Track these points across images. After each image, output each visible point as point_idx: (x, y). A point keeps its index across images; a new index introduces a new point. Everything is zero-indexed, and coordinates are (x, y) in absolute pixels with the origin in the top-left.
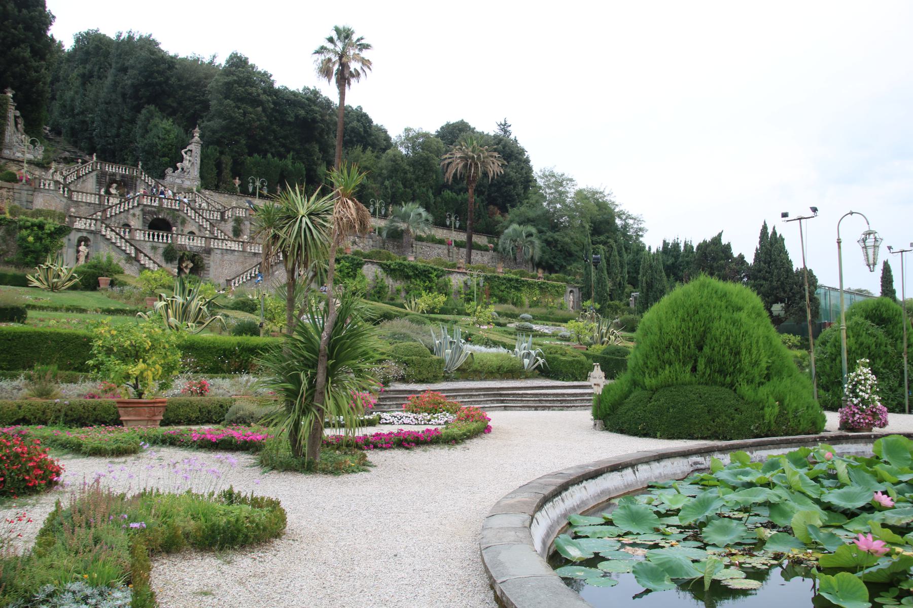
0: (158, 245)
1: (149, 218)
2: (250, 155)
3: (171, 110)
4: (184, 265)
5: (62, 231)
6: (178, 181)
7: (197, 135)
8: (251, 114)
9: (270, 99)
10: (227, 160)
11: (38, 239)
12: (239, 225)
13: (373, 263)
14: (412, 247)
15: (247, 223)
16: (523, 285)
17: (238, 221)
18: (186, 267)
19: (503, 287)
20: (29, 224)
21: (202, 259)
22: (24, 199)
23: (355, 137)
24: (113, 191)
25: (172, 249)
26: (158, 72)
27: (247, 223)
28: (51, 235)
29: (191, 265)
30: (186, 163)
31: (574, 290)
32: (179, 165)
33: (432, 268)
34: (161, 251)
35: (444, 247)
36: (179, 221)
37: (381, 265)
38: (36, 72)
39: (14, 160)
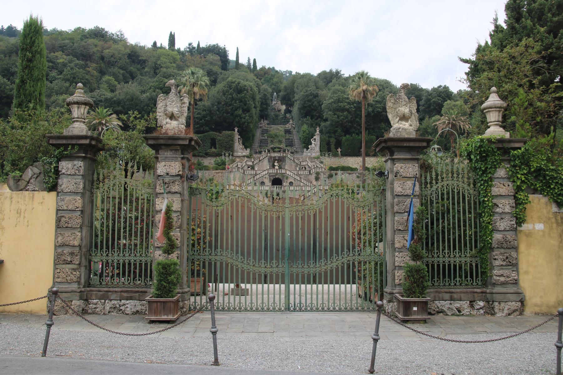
1: (272, 178)
6: (309, 154)
7: (318, 131)
8: (341, 116)
9: (352, 106)
10: (333, 140)
12: (318, 175)
15: (322, 174)
17: (318, 174)
24: (276, 164)
26: (309, 101)
27: (322, 174)
30: (313, 145)
32: (309, 146)
36: (285, 178)
38: (244, 118)
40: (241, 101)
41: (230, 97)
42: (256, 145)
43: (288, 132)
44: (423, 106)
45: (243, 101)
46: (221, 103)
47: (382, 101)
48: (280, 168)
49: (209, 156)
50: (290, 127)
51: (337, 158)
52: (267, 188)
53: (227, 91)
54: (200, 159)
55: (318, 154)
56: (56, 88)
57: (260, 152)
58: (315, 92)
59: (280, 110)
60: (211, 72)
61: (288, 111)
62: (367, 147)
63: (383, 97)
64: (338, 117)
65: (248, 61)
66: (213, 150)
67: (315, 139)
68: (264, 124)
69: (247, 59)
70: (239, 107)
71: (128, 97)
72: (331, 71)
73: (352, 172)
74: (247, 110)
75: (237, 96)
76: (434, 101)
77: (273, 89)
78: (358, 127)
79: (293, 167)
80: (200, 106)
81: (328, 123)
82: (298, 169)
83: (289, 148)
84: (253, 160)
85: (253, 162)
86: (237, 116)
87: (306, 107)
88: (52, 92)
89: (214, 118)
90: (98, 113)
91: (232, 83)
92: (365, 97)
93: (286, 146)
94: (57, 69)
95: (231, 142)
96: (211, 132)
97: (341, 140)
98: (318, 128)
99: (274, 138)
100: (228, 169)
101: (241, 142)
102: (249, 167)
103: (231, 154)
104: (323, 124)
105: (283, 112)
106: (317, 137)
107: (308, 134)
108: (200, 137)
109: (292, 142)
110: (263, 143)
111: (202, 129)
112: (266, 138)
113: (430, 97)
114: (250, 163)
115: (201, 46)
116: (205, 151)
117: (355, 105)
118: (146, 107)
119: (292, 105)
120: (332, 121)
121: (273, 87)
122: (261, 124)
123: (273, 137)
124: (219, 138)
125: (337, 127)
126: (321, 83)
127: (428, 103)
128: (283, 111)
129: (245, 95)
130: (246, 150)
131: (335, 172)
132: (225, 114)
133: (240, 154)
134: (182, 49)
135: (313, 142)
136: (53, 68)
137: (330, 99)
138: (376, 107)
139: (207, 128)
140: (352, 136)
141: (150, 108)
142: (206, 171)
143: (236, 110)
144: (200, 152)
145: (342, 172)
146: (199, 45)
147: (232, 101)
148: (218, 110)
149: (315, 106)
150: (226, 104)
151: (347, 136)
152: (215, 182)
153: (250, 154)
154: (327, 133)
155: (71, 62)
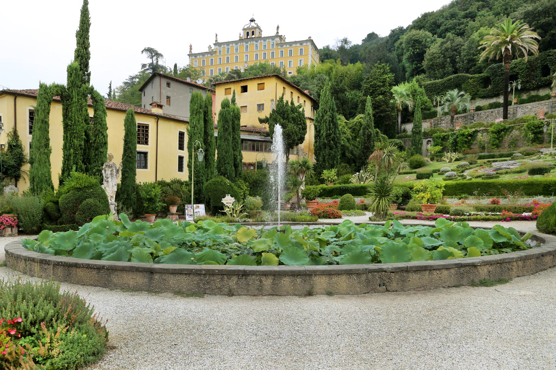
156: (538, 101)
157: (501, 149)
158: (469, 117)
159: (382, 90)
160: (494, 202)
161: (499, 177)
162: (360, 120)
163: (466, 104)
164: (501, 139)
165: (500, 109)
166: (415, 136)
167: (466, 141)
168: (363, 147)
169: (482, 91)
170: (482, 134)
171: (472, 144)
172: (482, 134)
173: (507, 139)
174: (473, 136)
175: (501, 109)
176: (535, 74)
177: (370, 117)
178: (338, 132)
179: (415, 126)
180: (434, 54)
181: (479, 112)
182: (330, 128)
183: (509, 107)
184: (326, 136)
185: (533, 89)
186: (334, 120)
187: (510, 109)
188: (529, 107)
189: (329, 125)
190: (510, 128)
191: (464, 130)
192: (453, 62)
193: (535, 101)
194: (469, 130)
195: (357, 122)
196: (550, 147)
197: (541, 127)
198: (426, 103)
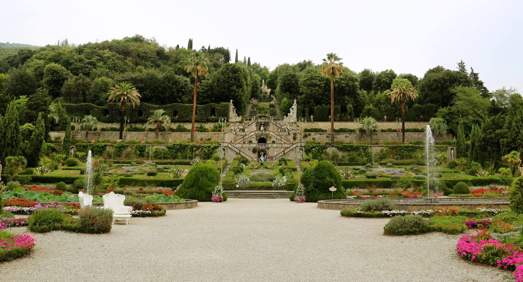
0: (250, 148)
1: (258, 138)
2: (317, 106)
3: (294, 93)
4: (261, 154)
5: (216, 147)
6: (288, 120)
7: (295, 102)
9: (322, 82)
10: (307, 109)
11: (208, 150)
13: (332, 146)
14: (377, 135)
16: (417, 149)
18: (262, 154)
19: (403, 151)
20: (206, 146)
21: (266, 151)
22: (222, 137)
23: (385, 84)
25: (255, 149)
26: (288, 80)
27: (299, 135)
28: (213, 149)
29: (263, 153)
30: (291, 113)
31: (454, 148)
32: (288, 114)
33: (361, 146)
34: (251, 150)
35: (395, 133)
37: (336, 147)
39: (232, 122)
40: (235, 80)
41: (227, 76)
42: (247, 115)
43: (272, 106)
44: (375, 84)
45: (237, 79)
46: (220, 81)
47: (346, 79)
48: (265, 130)
49: (209, 122)
50: (274, 103)
51: (310, 123)
52: (255, 146)
53: (225, 72)
54: (203, 124)
55: (296, 120)
56: (99, 73)
57: (250, 120)
58: (293, 74)
59: (267, 93)
60: (217, 65)
61: (272, 93)
62: (335, 115)
63: (346, 76)
64: (311, 91)
65: (245, 59)
66: (213, 117)
67: (293, 108)
68: (254, 101)
69: (244, 58)
70: (234, 84)
71: (149, 76)
72: (305, 61)
73: (323, 133)
74: (240, 86)
75: (233, 75)
76: (383, 81)
77: (262, 78)
78: (327, 99)
79: (276, 130)
80: (204, 83)
81: (304, 96)
82: (279, 131)
83: (273, 117)
84: (243, 125)
85: (244, 126)
86: (232, 91)
87: (286, 85)
88: (96, 76)
89: (215, 92)
90: (122, 86)
91: (229, 65)
92: (333, 74)
93: (270, 116)
94: (103, 61)
95: (227, 111)
96: (211, 104)
97: (314, 109)
98: (295, 100)
99: (261, 110)
100: (223, 131)
101: (235, 111)
102: (240, 130)
103: (226, 119)
104: (299, 97)
105: (268, 94)
106: (295, 107)
107: (288, 105)
108: (203, 107)
109: (275, 113)
110: (252, 113)
111: (205, 101)
112: (255, 110)
113: (380, 78)
114: (242, 127)
115: (211, 48)
116: (207, 118)
117: (324, 82)
118: (162, 85)
119: (275, 88)
120: (306, 93)
121: (262, 76)
122: (252, 101)
123: (261, 110)
124: (218, 107)
125: (310, 99)
126: (298, 69)
127: (379, 82)
128: (269, 93)
129: (239, 74)
130: (239, 117)
131: (309, 133)
132: (223, 90)
133: (234, 120)
134: (197, 50)
135: (291, 111)
136: (100, 60)
137: (304, 77)
138: (341, 83)
139: (208, 100)
140: (322, 106)
141: (165, 85)
142: (206, 133)
143: (232, 86)
144: (202, 119)
145: (315, 133)
146: (209, 47)
147: (228, 79)
148: (218, 86)
149: (293, 84)
150: (224, 81)
151: (318, 106)
152: (212, 141)
153: (241, 120)
154: (302, 104)
155: (113, 56)
156: (138, 131)
157: (121, 158)
158: (97, 134)
159: (44, 108)
160: (141, 189)
161: (132, 176)
162: (28, 127)
163: (97, 126)
164: (121, 152)
165: (117, 132)
166: (66, 143)
167: (99, 151)
168: (35, 148)
169: (103, 117)
170: (110, 147)
171: (103, 153)
172: (110, 147)
173: (125, 152)
174: (104, 147)
175: (119, 132)
176: (135, 114)
177: (43, 129)
178: (19, 136)
179: (67, 136)
180: (71, 85)
181: (104, 132)
182: (14, 132)
183: (123, 132)
184: (10, 138)
185: (134, 123)
186: (17, 127)
187: (124, 132)
188: (134, 134)
189: (14, 130)
190: (126, 146)
191: (98, 144)
192: (84, 94)
193: (137, 131)
194: (102, 144)
195: (26, 129)
196: (149, 160)
197: (143, 148)
198: (67, 119)
